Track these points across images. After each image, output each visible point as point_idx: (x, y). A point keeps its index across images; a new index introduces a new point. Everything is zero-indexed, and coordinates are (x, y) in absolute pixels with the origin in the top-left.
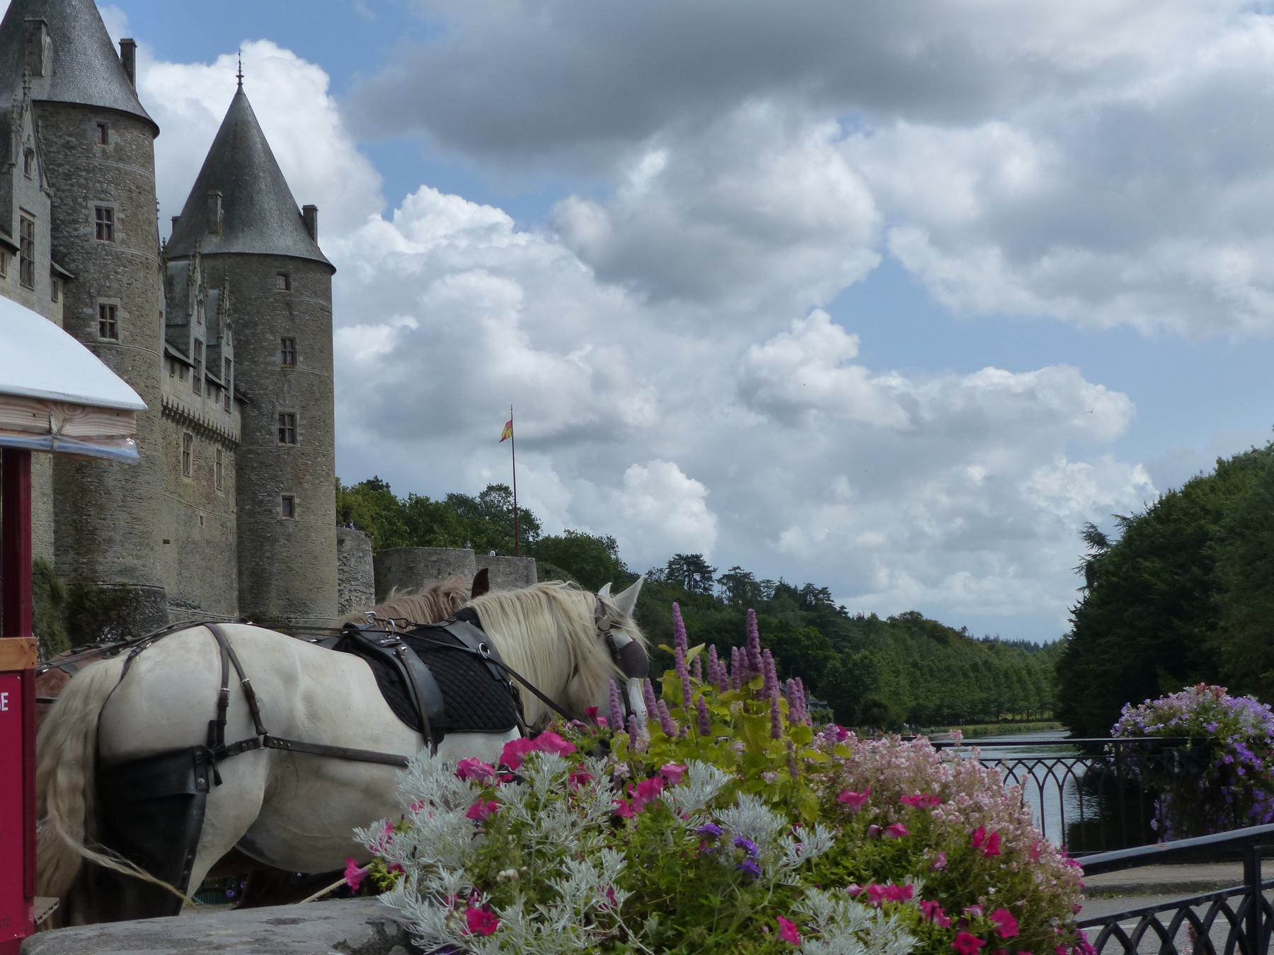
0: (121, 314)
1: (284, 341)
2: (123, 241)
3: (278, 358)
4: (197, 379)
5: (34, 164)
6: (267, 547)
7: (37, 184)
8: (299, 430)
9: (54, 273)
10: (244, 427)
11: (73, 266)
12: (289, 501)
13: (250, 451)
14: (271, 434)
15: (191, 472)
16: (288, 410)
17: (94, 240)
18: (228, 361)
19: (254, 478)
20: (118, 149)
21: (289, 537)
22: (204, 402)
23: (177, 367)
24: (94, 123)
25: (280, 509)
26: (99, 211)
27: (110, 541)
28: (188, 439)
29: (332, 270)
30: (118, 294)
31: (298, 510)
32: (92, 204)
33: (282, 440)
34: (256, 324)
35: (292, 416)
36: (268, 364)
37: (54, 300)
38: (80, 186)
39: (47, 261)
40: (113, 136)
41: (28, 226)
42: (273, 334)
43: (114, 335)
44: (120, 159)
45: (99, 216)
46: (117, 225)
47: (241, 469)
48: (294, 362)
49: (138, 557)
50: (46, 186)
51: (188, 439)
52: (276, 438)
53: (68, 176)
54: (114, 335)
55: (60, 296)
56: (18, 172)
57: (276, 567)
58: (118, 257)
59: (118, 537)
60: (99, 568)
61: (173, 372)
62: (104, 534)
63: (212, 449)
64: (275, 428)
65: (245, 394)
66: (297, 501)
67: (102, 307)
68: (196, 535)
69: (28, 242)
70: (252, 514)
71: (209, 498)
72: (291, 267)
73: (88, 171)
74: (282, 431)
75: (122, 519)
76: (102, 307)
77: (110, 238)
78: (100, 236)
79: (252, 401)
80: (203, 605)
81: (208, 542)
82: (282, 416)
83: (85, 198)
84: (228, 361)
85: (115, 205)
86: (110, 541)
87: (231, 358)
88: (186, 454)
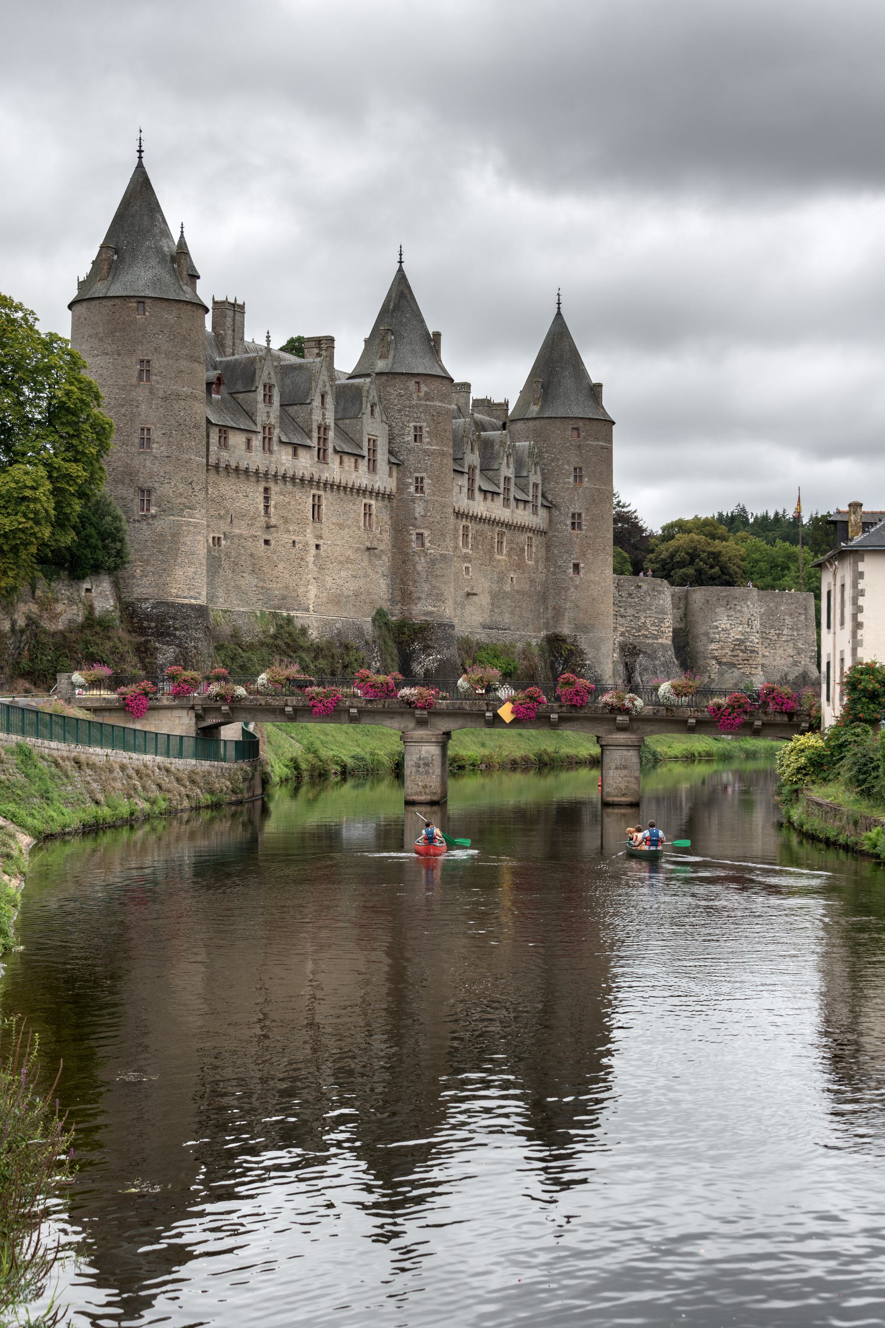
0: (427, 481)
1: (575, 469)
2: (428, 443)
3: (571, 480)
4: (506, 500)
5: (377, 410)
6: (563, 593)
7: (379, 420)
8: (583, 523)
9: (390, 462)
10: (550, 521)
11: (401, 458)
12: (576, 567)
13: (554, 536)
14: (567, 526)
15: (505, 552)
16: (577, 511)
17: (413, 444)
18: (536, 485)
19: (556, 552)
20: (426, 394)
21: (576, 587)
22: (513, 512)
23: (489, 496)
24: (413, 382)
25: (571, 570)
26: (415, 427)
27: (419, 598)
28: (501, 534)
29: (614, 423)
30: (426, 470)
31: (582, 572)
32: (411, 425)
33: (574, 529)
34: (559, 460)
35: (580, 515)
36: (565, 483)
37: (390, 475)
38: (406, 415)
39: (386, 456)
40: (424, 388)
41: (373, 442)
42: (569, 465)
43: (423, 492)
44: (427, 400)
45: (415, 430)
46: (425, 434)
47: (548, 547)
48: (581, 481)
49: (435, 606)
50: (385, 419)
51: (501, 534)
52: (569, 528)
53: (399, 411)
54: (423, 492)
55: (395, 474)
56: (366, 418)
57: (568, 605)
58: (425, 451)
59: (423, 596)
60: (414, 612)
61: (485, 498)
62: (416, 595)
63: (523, 537)
64: (569, 522)
65: (551, 502)
66: (582, 565)
67: (417, 478)
68: (507, 588)
69: (373, 451)
70: (554, 573)
71: (520, 566)
72: (580, 424)
73: (410, 407)
74: (573, 524)
75: (426, 587)
76: (417, 478)
77: (421, 441)
78: (415, 440)
79: (555, 506)
80: (512, 628)
81: (518, 592)
82: (573, 515)
83: (408, 422)
84: (536, 485)
85: (424, 424)
86: (419, 598)
87: (539, 482)
88: (500, 543)
